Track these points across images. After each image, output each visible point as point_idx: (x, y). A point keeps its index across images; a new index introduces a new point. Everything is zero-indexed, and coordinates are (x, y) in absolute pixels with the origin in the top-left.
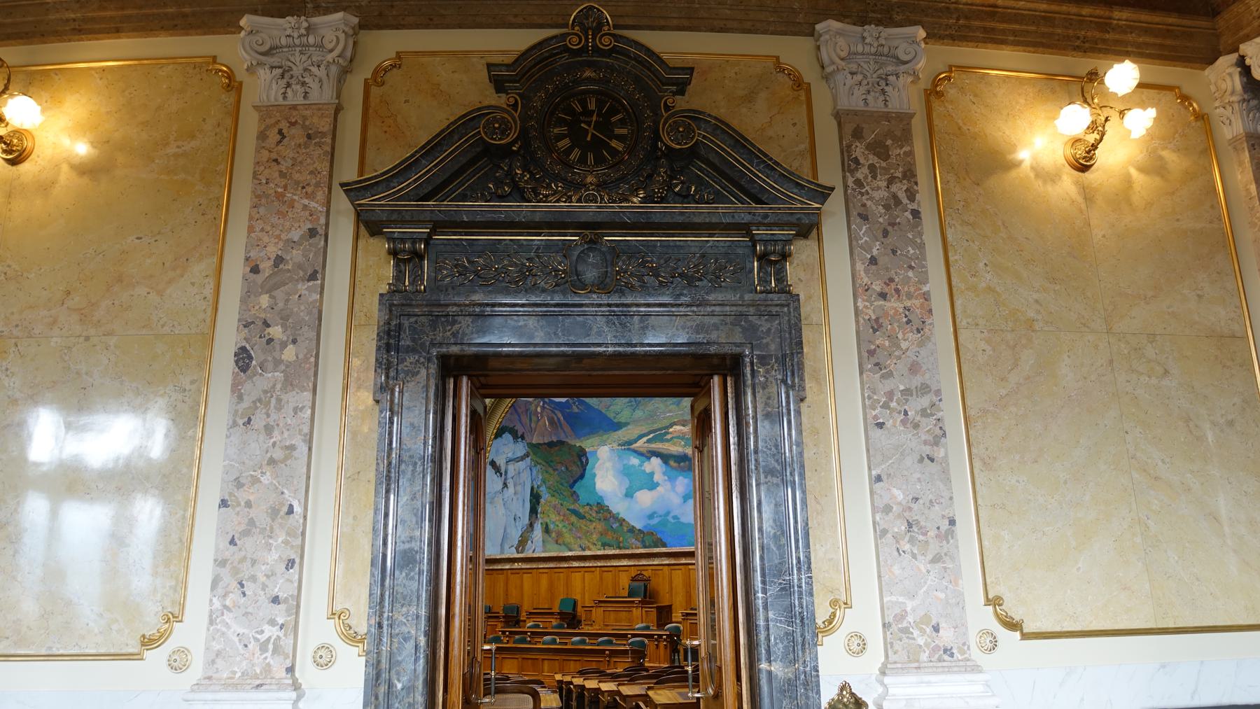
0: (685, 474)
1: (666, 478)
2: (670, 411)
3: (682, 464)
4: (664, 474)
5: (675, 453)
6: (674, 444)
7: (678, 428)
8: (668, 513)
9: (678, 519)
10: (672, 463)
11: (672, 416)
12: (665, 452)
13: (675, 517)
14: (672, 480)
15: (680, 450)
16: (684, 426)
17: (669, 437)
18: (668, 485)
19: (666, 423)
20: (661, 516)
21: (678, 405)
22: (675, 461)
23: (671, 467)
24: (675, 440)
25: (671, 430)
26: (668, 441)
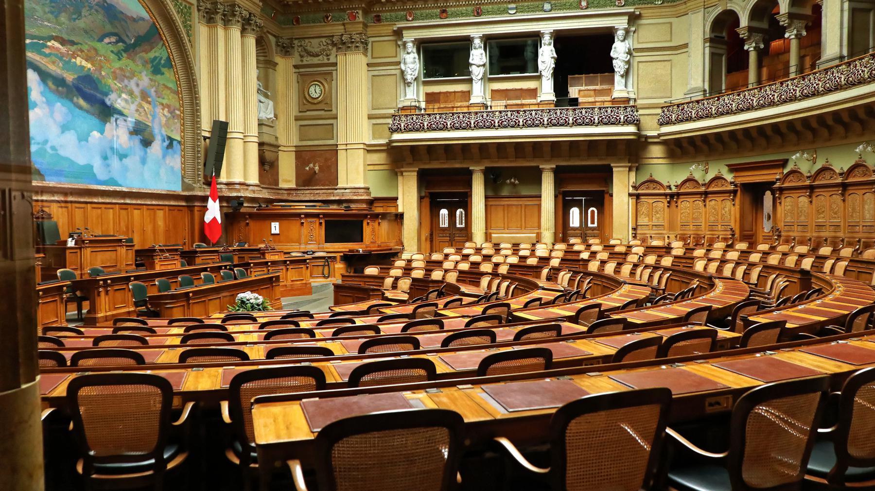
0: (62, 100)
1: (44, 99)
2: (49, 21)
3: (60, 88)
4: (42, 94)
5: (53, 73)
6: (54, 63)
7: (57, 45)
8: (46, 142)
9: (56, 150)
10: (50, 83)
11: (50, 27)
12: (43, 68)
13: (53, 148)
14: (49, 103)
15: (59, 71)
16: (62, 45)
17: (47, 51)
18: (47, 109)
19: (44, 32)
20: (38, 144)
21: (56, 17)
22: (53, 83)
23: (50, 88)
24: (54, 58)
25: (49, 44)
26: (46, 56)
